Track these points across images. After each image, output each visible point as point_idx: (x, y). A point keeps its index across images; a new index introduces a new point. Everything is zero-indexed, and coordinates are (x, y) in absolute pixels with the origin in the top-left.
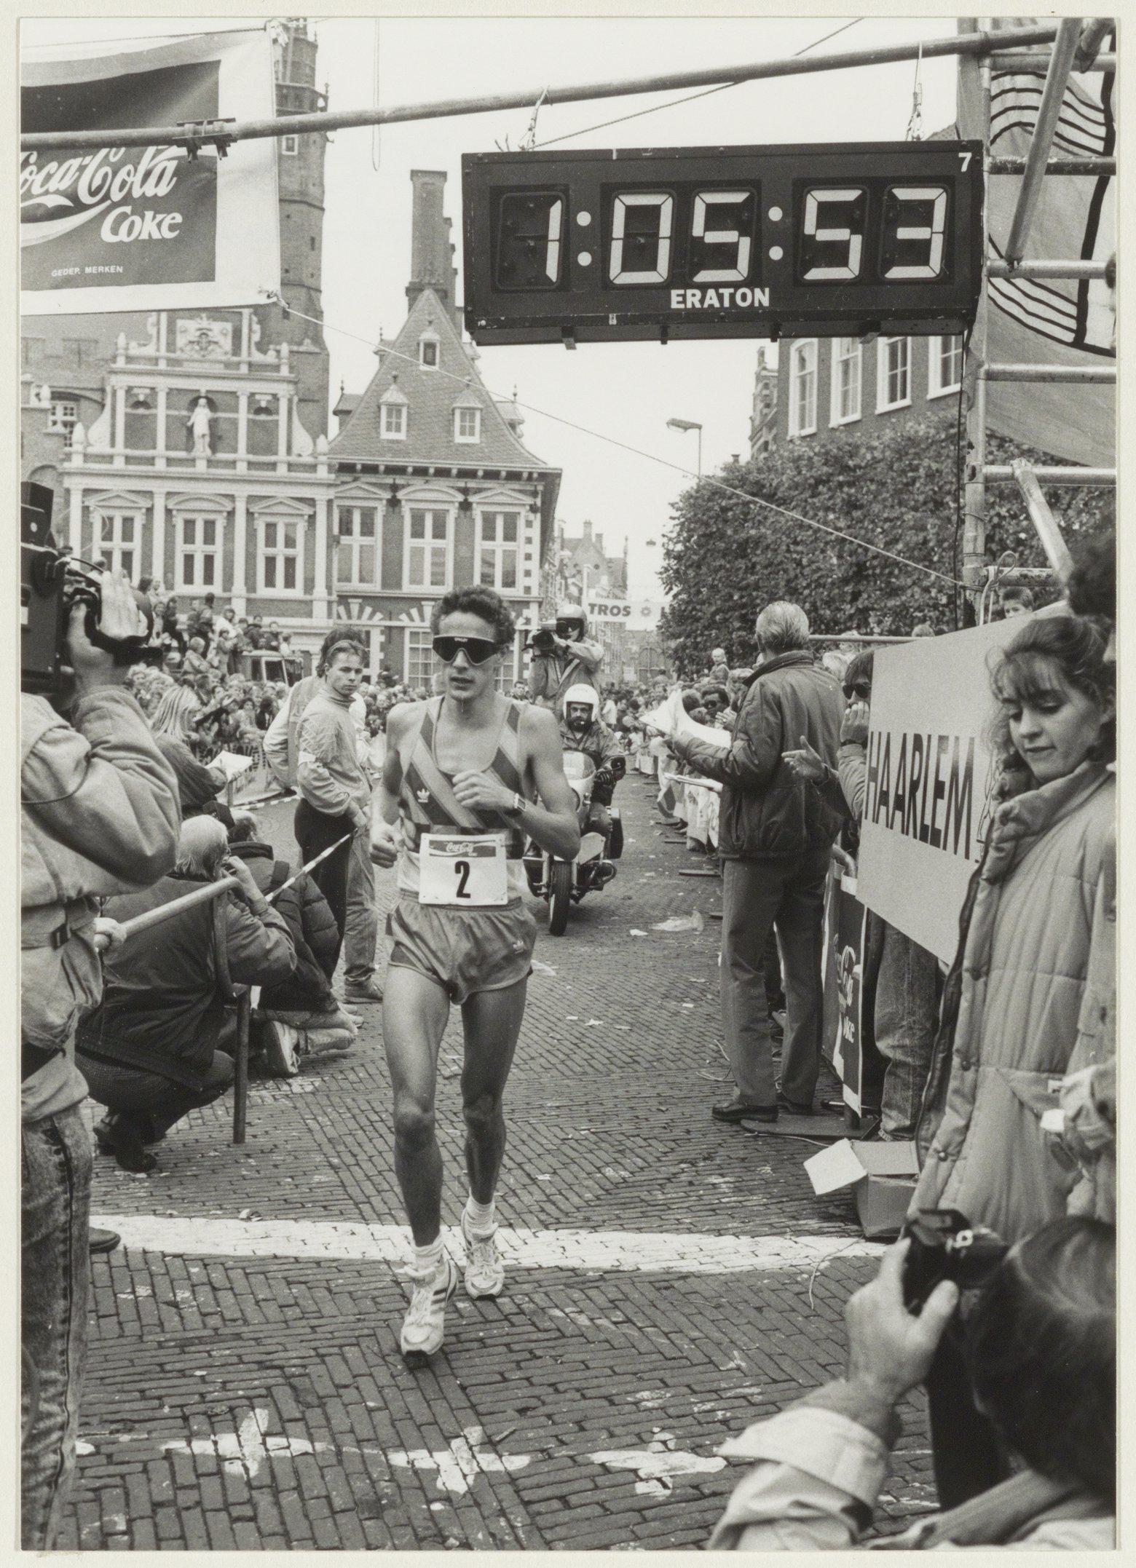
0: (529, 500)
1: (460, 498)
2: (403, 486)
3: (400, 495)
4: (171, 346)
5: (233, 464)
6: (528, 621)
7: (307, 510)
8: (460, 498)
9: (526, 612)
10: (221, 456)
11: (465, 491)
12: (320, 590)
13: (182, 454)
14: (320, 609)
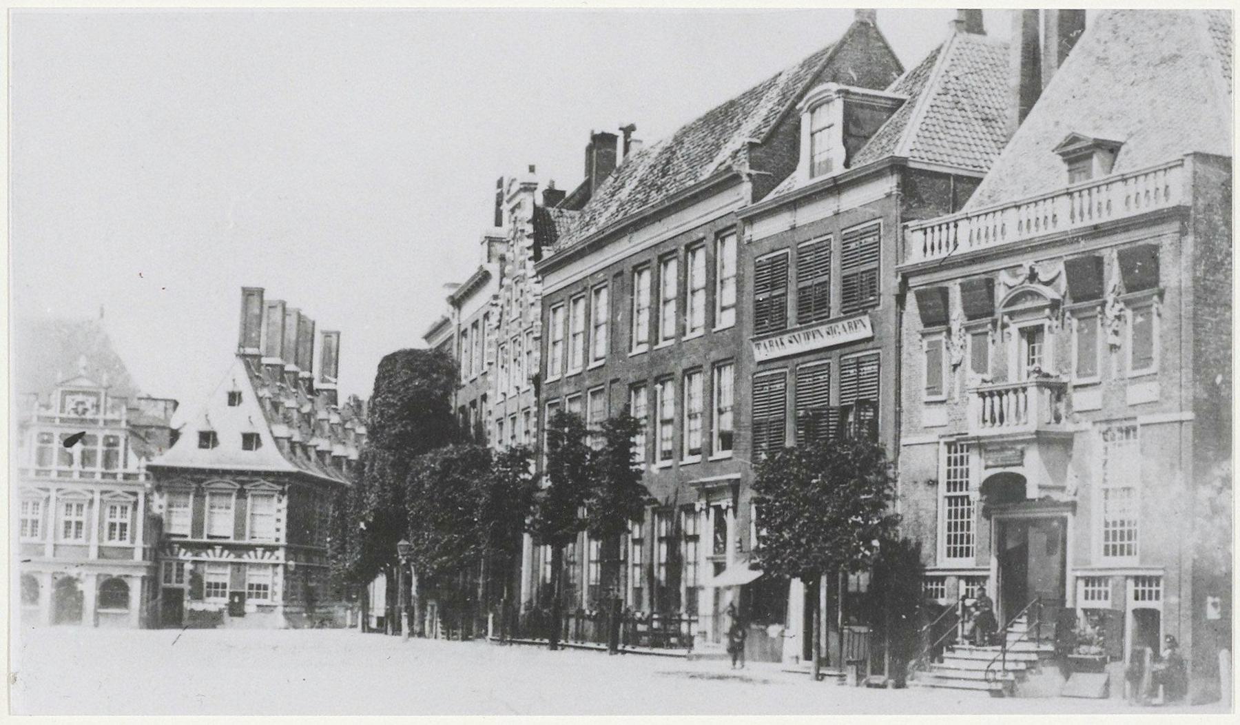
0: (280, 488)
1: (238, 486)
2: (205, 480)
3: (203, 485)
4: (62, 411)
5: (93, 474)
6: (277, 558)
7: (132, 499)
8: (238, 486)
9: (277, 553)
10: (88, 469)
11: (242, 483)
12: (139, 542)
13: (66, 468)
14: (138, 555)
